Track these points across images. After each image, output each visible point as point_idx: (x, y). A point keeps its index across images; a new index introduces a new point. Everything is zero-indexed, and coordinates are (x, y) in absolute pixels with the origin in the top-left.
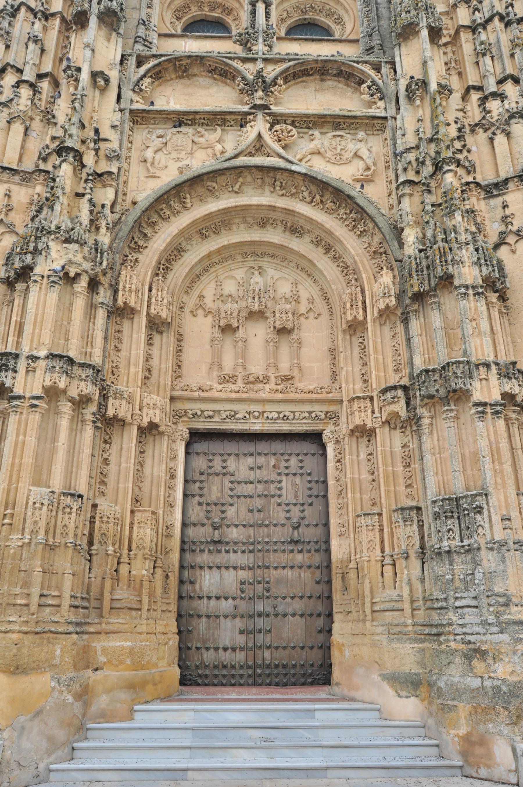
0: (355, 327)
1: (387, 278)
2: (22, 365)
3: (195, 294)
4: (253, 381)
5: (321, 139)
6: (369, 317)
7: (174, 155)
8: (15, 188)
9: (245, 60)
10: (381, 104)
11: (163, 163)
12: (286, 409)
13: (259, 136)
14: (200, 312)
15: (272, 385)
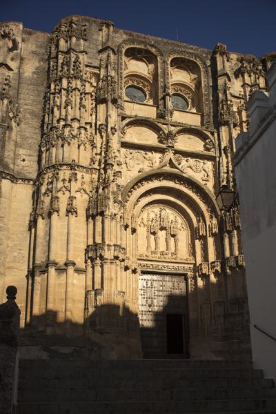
0: (204, 239)
1: (215, 221)
2: (106, 248)
3: (141, 217)
4: (162, 254)
5: (192, 161)
6: (208, 235)
7: (137, 162)
8: (84, 174)
9: (163, 124)
10: (213, 150)
11: (132, 165)
12: (176, 265)
13: (170, 160)
14: (142, 225)
15: (170, 256)
